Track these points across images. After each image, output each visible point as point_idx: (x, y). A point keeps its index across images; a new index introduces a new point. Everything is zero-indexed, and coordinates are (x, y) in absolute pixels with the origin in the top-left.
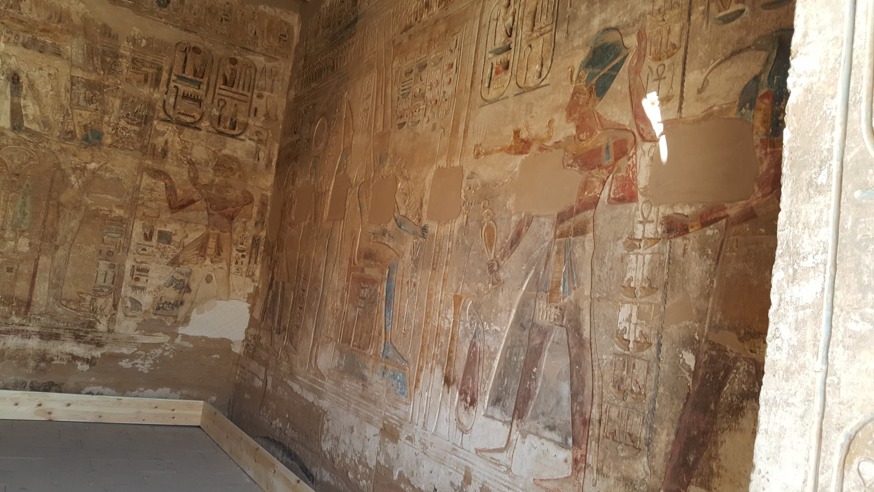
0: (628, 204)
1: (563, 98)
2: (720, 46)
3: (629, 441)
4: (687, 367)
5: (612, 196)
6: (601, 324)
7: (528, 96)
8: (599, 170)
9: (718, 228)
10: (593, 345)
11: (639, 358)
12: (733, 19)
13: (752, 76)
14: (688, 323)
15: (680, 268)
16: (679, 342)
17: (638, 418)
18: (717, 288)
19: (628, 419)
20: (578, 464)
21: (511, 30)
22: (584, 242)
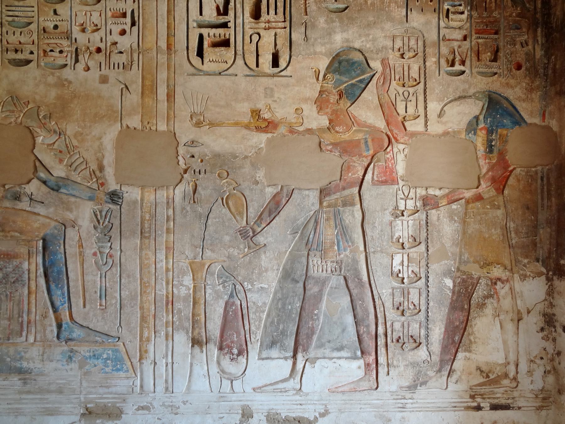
2: (451, 90)
4: (448, 287)
6: (378, 270)
9: (459, 205)
10: (373, 286)
11: (414, 288)
12: (459, 76)
13: (475, 115)
14: (446, 262)
15: (436, 228)
16: (441, 273)
17: (417, 324)
18: (462, 240)
22: (353, 211)
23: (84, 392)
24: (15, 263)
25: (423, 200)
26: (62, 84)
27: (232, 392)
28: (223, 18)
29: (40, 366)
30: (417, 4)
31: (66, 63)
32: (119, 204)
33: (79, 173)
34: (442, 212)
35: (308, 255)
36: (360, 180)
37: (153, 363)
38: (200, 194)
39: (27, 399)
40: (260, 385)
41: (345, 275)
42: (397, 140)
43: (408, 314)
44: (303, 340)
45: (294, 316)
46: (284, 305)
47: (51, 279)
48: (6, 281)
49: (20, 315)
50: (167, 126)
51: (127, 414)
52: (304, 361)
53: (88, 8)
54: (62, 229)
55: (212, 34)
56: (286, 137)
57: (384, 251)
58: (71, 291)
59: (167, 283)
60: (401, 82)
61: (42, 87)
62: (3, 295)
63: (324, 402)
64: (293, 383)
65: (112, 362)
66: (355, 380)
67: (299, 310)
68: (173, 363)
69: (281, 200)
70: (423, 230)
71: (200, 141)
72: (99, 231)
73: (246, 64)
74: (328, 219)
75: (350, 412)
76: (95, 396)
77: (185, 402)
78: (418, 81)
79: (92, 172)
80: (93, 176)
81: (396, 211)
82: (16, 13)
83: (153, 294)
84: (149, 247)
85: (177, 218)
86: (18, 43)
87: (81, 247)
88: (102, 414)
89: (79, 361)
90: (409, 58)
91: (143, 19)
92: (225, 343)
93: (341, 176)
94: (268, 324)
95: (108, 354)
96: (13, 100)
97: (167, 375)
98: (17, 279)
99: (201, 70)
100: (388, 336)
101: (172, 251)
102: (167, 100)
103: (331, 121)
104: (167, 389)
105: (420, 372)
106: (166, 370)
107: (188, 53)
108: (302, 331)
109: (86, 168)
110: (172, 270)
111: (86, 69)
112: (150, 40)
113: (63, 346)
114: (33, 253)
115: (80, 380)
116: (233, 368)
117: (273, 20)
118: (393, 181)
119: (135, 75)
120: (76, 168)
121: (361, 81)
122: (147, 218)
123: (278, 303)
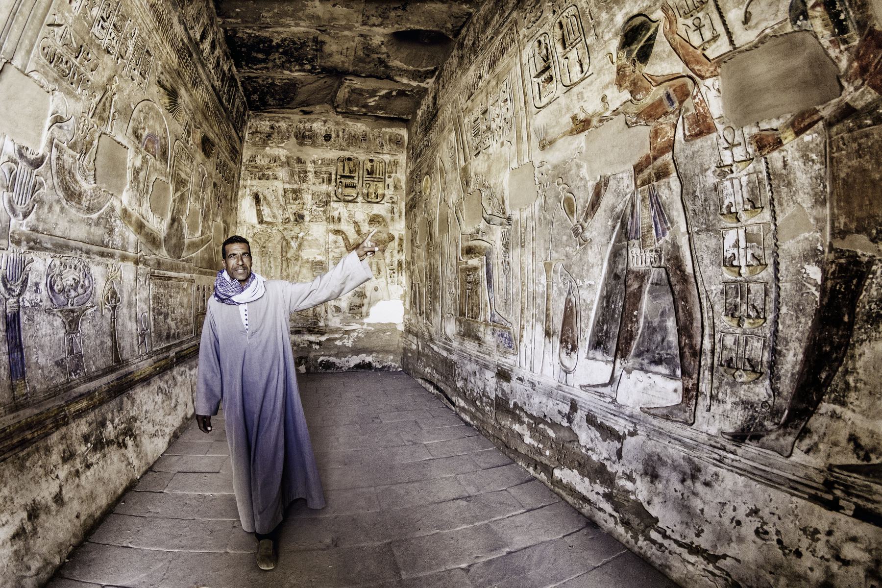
0: (707, 136)
1: (611, 75)
3: (748, 367)
4: (812, 281)
5: (687, 134)
6: (705, 256)
7: (575, 90)
10: (699, 279)
11: (755, 282)
14: (807, 235)
16: (800, 257)
18: (832, 193)
19: (746, 345)
20: (690, 394)
21: (547, 57)
25: (757, 142)
34: (790, 152)
70: (765, 188)
74: (643, 200)
105: (753, 418)
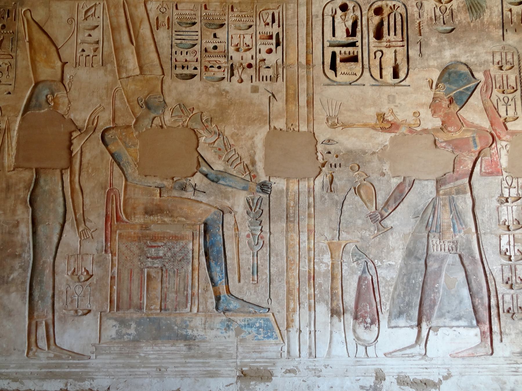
6: (489, 249)
8: (469, 154)
22: (465, 198)
23: (240, 357)
24: (181, 244)
26: (220, 93)
27: (366, 356)
28: (352, 39)
29: (203, 333)
30: (512, 25)
31: (223, 76)
32: (268, 193)
33: (235, 167)
35: (428, 236)
36: (470, 172)
37: (298, 331)
38: (336, 184)
39: (191, 363)
40: (391, 351)
41: (460, 253)
42: (500, 138)
43: (516, 288)
44: (426, 311)
45: (417, 289)
46: (409, 280)
47: (211, 258)
48: (174, 260)
49: (186, 289)
50: (307, 127)
51: (276, 376)
52: (428, 330)
53: (242, 32)
54: (220, 214)
55: (343, 52)
56: (407, 136)
57: (493, 232)
58: (228, 268)
59: (309, 261)
60: (502, 90)
61: (204, 96)
62: (171, 271)
63: (447, 366)
64: (419, 349)
65: (264, 330)
66: (473, 346)
67: (421, 284)
68: (315, 331)
69: (404, 189)
71: (335, 139)
72: (252, 216)
73: (371, 75)
74: (444, 205)
75: (469, 375)
76: (249, 360)
77: (326, 366)
78: (515, 89)
79: (245, 166)
80: (246, 170)
81: (501, 198)
82: (184, 37)
83: (298, 271)
84: (294, 230)
85: (317, 205)
86: (185, 61)
87: (236, 230)
88: (255, 377)
89: (235, 329)
90: (507, 70)
91: (286, 40)
92: (359, 314)
93: (454, 168)
94: (395, 296)
95: (260, 323)
96: (180, 107)
97: (310, 342)
98: (183, 258)
99: (334, 81)
100: (500, 307)
101: (313, 233)
102: (307, 106)
103: (443, 123)
104: (310, 354)
106: (310, 337)
107: (323, 68)
108: (425, 302)
109: (241, 163)
110: (313, 250)
111: (240, 81)
112: (292, 57)
113: (222, 316)
114: (196, 235)
115: (237, 346)
116: (368, 336)
117: (393, 40)
118: (499, 173)
119: (280, 86)
120: (232, 163)
121: (467, 89)
122: (292, 205)
123: (403, 278)
